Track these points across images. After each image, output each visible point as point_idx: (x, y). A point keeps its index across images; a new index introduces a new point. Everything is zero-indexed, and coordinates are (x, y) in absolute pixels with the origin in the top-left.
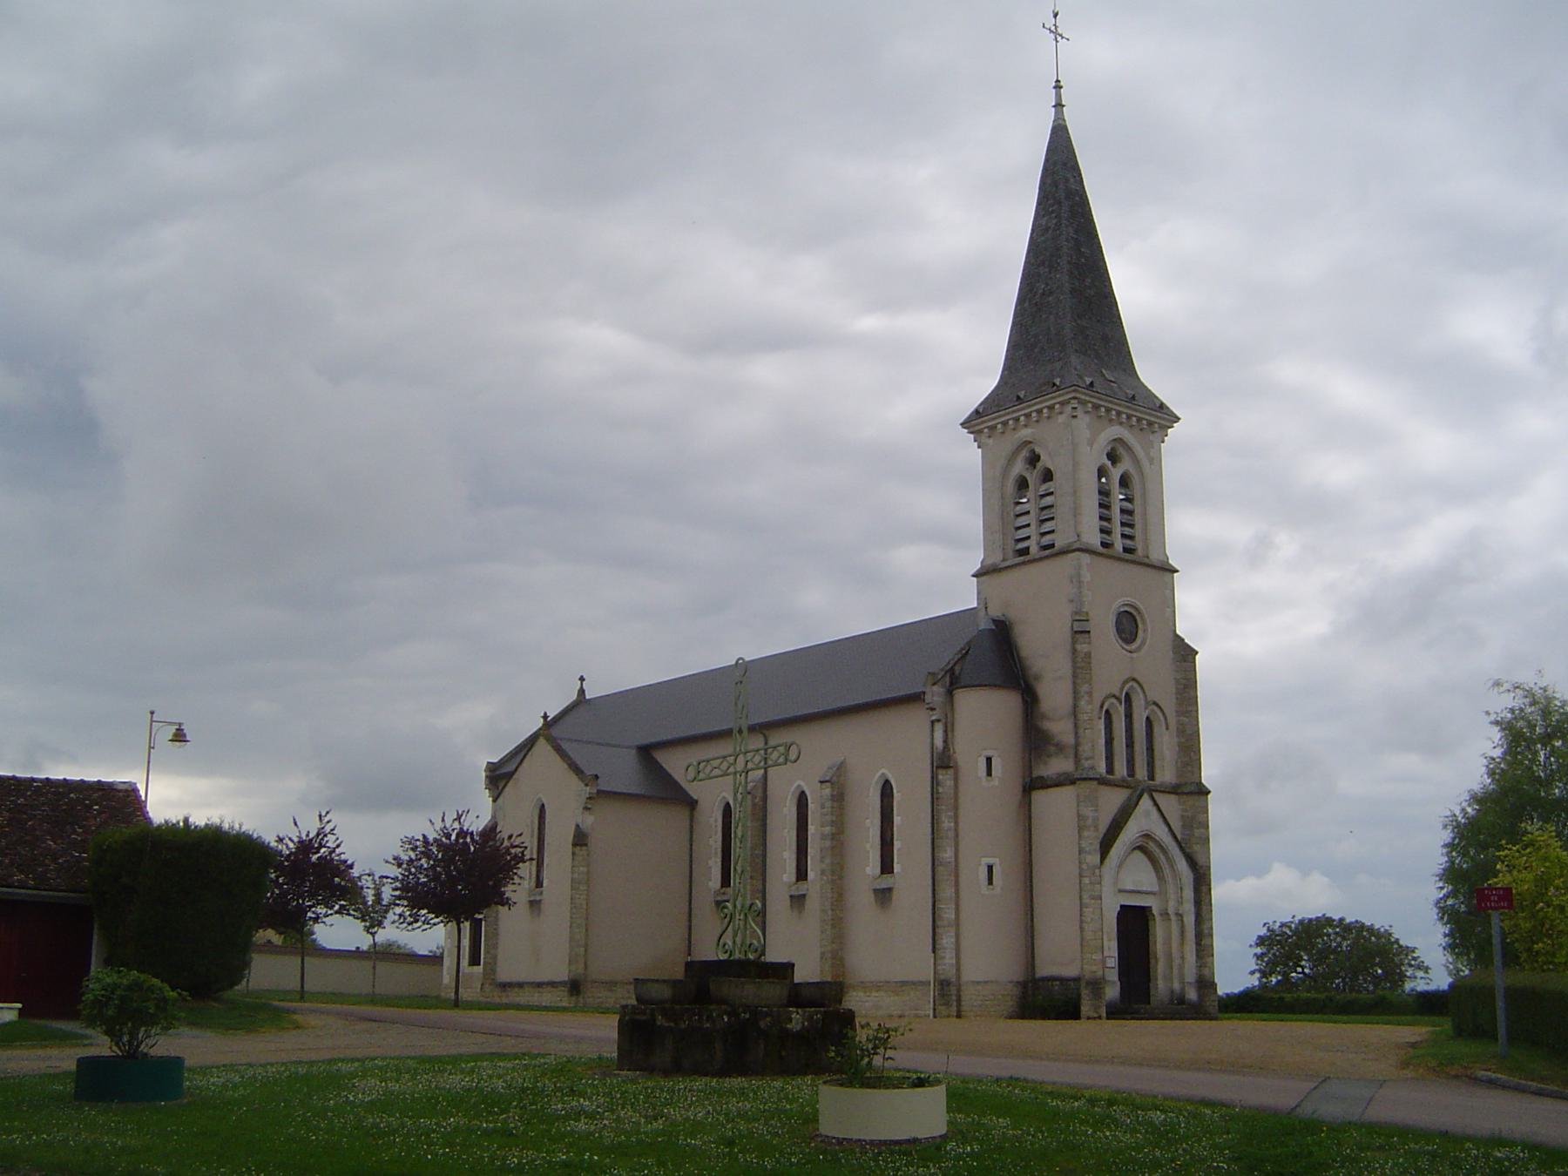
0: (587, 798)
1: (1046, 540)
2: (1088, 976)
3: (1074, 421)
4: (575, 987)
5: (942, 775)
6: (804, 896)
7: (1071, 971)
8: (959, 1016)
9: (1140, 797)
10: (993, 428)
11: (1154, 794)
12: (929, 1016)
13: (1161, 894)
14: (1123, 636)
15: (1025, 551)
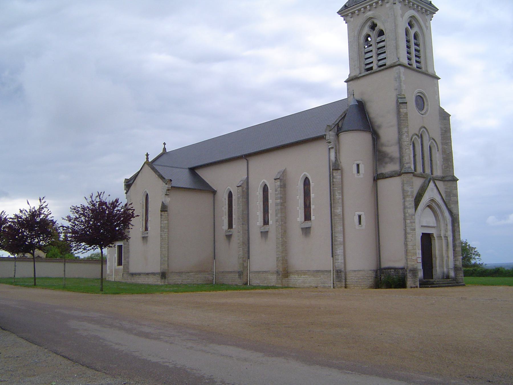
0: (167, 190)
1: (381, 63)
2: (410, 267)
3: (394, 5)
4: (163, 275)
5: (336, 173)
6: (267, 232)
7: (400, 264)
8: (346, 287)
9: (429, 182)
10: (353, 13)
11: (436, 182)
12: (331, 287)
13: (438, 227)
14: (418, 107)
15: (371, 68)
